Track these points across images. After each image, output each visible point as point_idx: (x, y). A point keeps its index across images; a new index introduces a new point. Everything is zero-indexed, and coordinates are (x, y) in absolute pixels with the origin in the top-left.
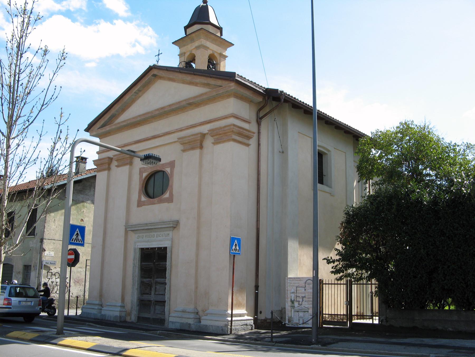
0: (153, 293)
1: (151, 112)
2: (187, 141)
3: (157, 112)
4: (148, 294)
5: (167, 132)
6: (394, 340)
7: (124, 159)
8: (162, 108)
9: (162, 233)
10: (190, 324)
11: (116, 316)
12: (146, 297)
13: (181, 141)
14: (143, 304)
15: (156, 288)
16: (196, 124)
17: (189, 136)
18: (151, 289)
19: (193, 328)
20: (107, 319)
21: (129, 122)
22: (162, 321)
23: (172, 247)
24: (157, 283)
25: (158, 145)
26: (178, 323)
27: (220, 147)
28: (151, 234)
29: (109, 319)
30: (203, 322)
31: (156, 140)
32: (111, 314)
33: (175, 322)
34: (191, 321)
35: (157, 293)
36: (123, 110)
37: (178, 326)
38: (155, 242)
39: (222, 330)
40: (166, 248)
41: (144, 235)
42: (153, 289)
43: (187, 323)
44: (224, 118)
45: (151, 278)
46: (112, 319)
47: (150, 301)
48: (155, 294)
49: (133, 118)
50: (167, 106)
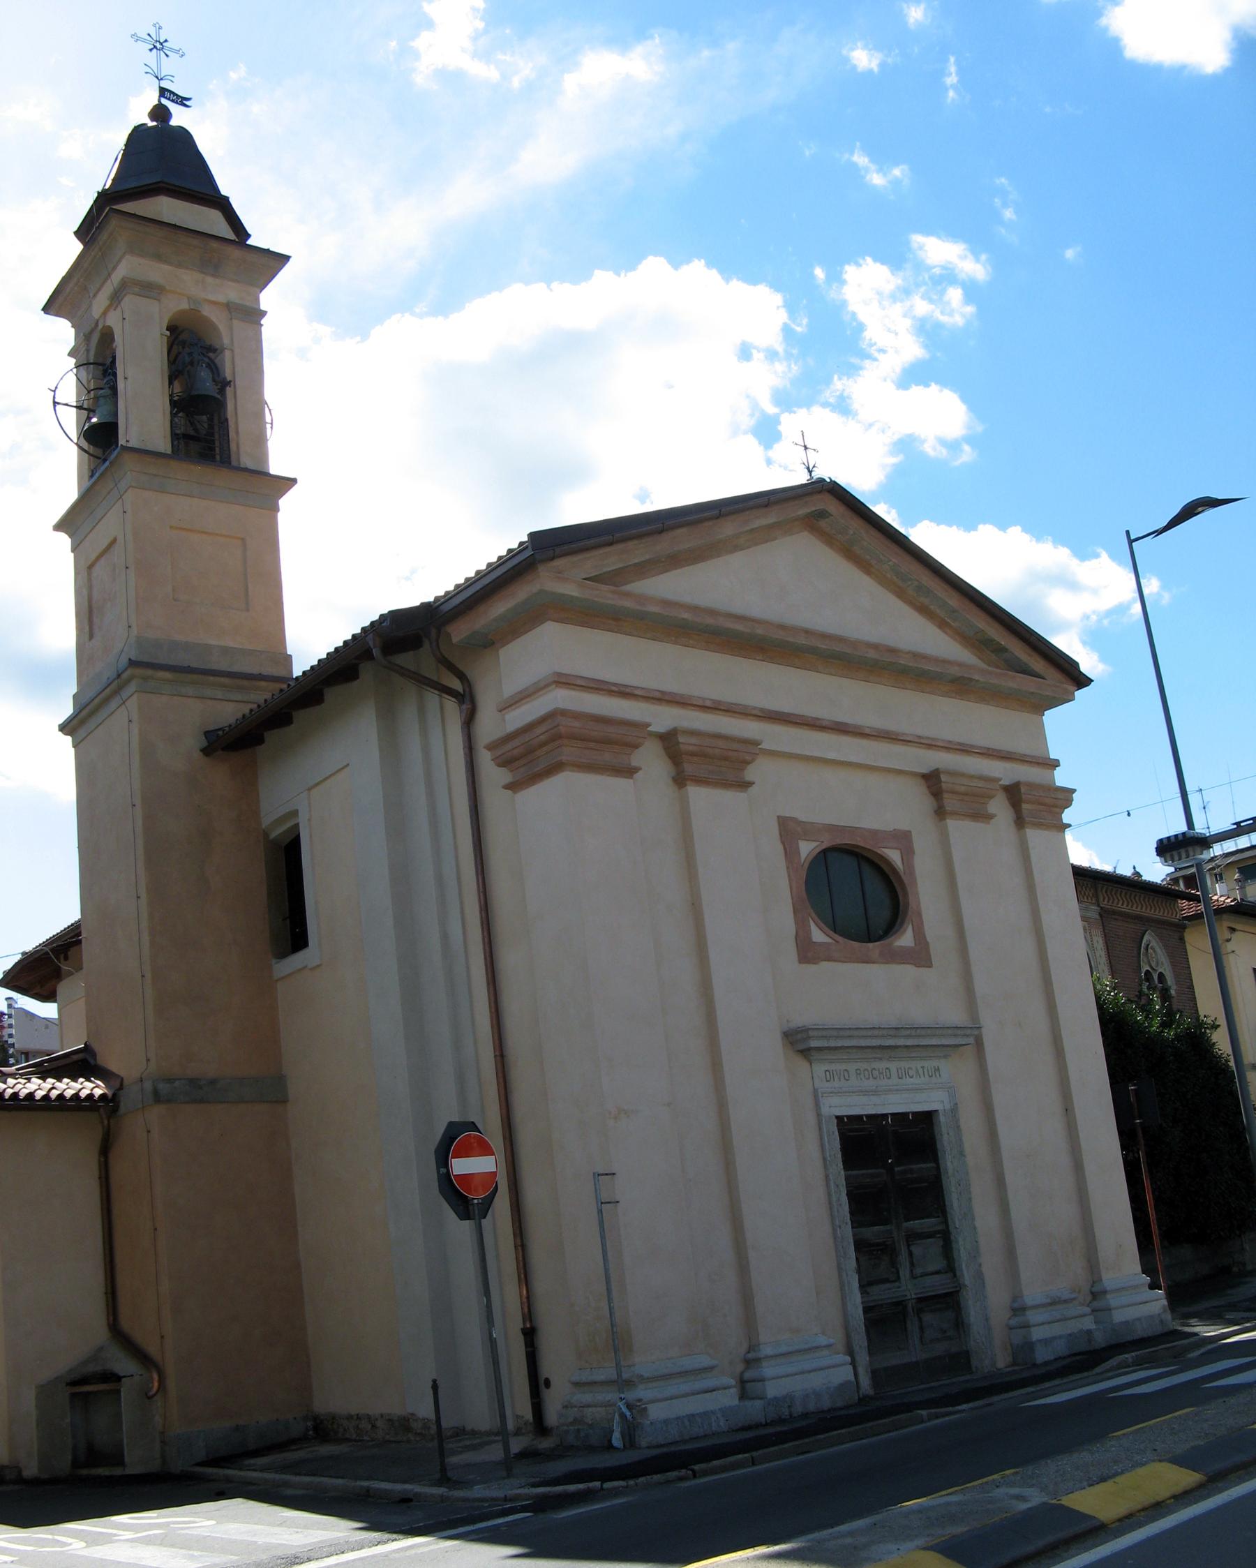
0: (905, 1273)
1: (855, 644)
2: (963, 789)
3: (872, 654)
4: (887, 1281)
5: (888, 732)
6: (665, 1450)
7: (726, 759)
8: (893, 651)
9: (918, 1064)
10: (1089, 1332)
11: (843, 1386)
12: (882, 1293)
13: (932, 781)
14: (883, 1322)
15: (911, 1254)
16: (972, 746)
17: (971, 777)
18: (894, 1264)
19: (1100, 1340)
20: (798, 1409)
21: (760, 631)
22: (961, 1360)
23: (954, 1110)
24: (913, 1237)
25: (852, 758)
26: (1060, 1337)
27: (533, 796)
28: (877, 1065)
29: (812, 1407)
30: (1119, 1317)
31: (845, 740)
32: (816, 1381)
33: (1054, 1338)
34: (1088, 1323)
35: (918, 1271)
36: (675, 561)
37: (1061, 1349)
38: (894, 1094)
39: (1162, 1321)
40: (927, 1118)
41: (852, 1067)
42: (903, 1258)
43: (1081, 1331)
44: (1038, 764)
45: (886, 1222)
46: (826, 1404)
47: (900, 1304)
48: (913, 1277)
49: (782, 627)
50: (908, 653)
